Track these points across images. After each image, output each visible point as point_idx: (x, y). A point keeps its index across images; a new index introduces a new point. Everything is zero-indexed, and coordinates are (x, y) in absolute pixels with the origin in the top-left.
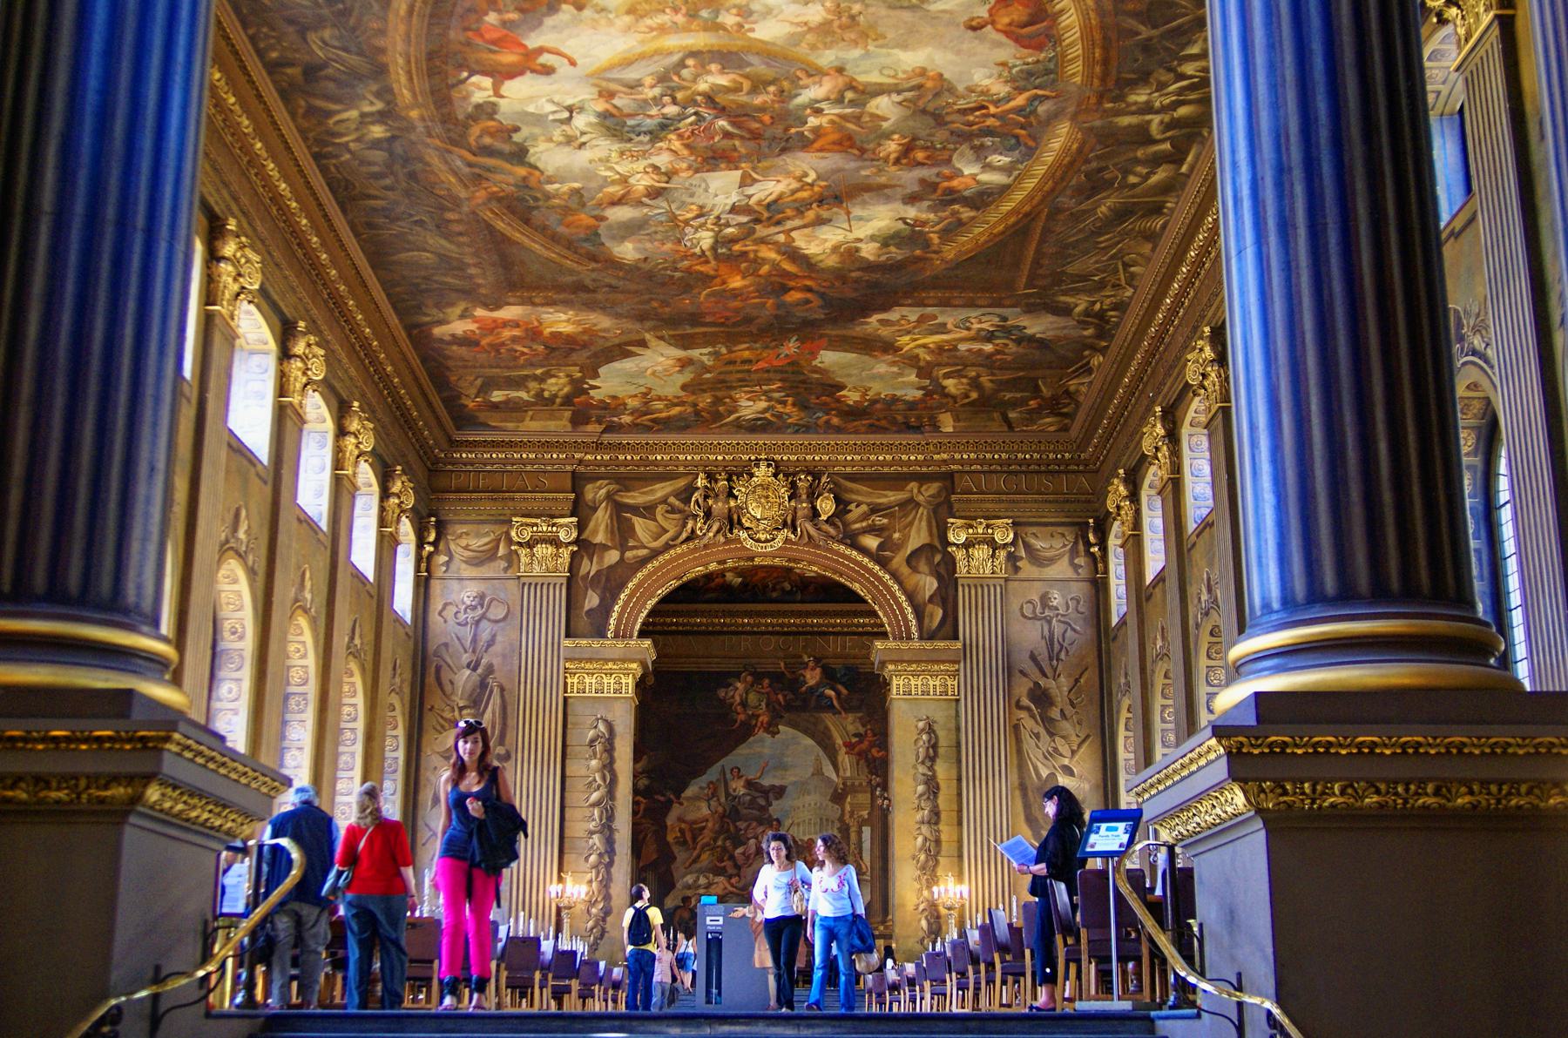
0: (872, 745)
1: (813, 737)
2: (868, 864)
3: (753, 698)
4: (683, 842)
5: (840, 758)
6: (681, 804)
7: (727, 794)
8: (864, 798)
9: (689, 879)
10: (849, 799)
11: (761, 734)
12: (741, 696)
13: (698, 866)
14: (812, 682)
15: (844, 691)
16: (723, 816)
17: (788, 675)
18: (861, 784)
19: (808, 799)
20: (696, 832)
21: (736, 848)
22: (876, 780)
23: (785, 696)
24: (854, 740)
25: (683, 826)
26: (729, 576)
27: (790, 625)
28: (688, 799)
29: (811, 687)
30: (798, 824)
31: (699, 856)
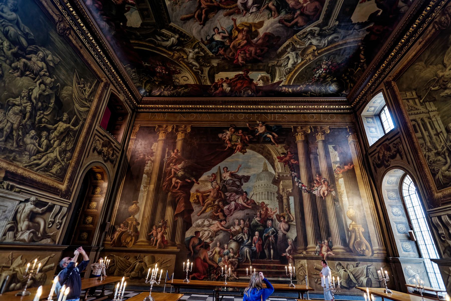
0: (291, 158)
1: (262, 154)
2: (294, 216)
3: (234, 138)
4: (197, 203)
5: (276, 164)
7: (221, 179)
8: (289, 182)
9: (200, 222)
10: (281, 183)
11: (238, 153)
12: (229, 137)
13: (204, 215)
14: (261, 132)
15: (276, 135)
16: (219, 190)
18: (287, 176)
19: (262, 182)
20: (205, 197)
21: (224, 205)
22: (295, 174)
23: (249, 137)
24: (282, 156)
25: (199, 194)
26: (225, 85)
27: (250, 109)
28: (202, 181)
29: (261, 134)
30: (256, 194)
31: (205, 210)
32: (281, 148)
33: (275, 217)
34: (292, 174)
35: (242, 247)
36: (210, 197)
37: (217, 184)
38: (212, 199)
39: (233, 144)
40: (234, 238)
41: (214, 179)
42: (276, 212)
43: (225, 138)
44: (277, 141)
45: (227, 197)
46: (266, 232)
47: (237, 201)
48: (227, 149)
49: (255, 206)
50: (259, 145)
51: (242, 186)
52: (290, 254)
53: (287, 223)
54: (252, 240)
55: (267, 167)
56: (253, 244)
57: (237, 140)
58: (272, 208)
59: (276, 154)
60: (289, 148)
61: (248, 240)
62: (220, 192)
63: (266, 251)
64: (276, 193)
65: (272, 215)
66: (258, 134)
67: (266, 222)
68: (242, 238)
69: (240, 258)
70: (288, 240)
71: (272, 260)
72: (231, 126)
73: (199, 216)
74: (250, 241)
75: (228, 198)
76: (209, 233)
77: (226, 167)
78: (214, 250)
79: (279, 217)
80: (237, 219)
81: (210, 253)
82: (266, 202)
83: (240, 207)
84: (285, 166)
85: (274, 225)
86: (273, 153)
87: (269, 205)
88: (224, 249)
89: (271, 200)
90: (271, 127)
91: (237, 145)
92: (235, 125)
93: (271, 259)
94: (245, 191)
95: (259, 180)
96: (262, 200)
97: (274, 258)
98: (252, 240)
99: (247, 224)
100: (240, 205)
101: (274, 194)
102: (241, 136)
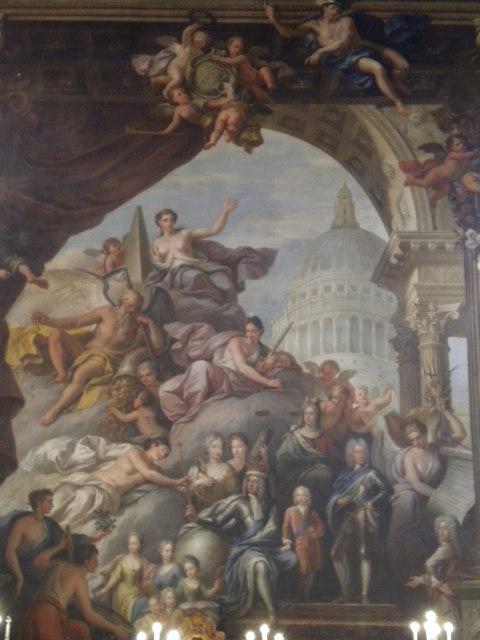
1: (332, 149)
2: (466, 420)
3: (206, 75)
4: (41, 367)
5: (393, 195)
6: (44, 285)
7: (147, 265)
9: (51, 450)
10: (415, 278)
12: (182, 71)
15: (401, 62)
16: (137, 310)
17: (281, 30)
18: (441, 248)
19: (326, 278)
21: (161, 378)
23: (274, 72)
25: (45, 331)
29: (330, 55)
30: (303, 329)
31: (76, 398)
32: (423, 120)
33: (380, 424)
34: (464, 239)
35: (235, 550)
36: (96, 343)
37: (130, 286)
38: (107, 350)
39: (200, 102)
40: (204, 515)
41: (114, 265)
42: (387, 403)
43: (162, 78)
44: (403, 88)
45: (174, 341)
46: (341, 489)
47: (216, 357)
48: (171, 127)
49: (293, 378)
50: (319, 109)
51: (241, 297)
52: (442, 578)
53: (433, 448)
54: (280, 522)
55: (352, 207)
56: (286, 541)
57: (221, 87)
58: (370, 386)
59: (394, 151)
60: (456, 120)
61: (264, 522)
62: (140, 318)
63: (341, 569)
64: (387, 325)
65: (370, 415)
66: (315, 57)
67: (341, 445)
68: (237, 513)
69: (227, 598)
70: (439, 519)
71: (365, 603)
72: (193, 20)
73: (47, 424)
74: (270, 526)
75: (177, 346)
76: (92, 499)
77: (169, 212)
78: (114, 567)
79: (399, 428)
80: (217, 435)
81: (98, 581)
82: (345, 362)
83: (230, 386)
84: (433, 206)
85: (376, 460)
86: (381, 144)
87: (353, 373)
88: (158, 561)
89: (365, 352)
90: (379, 20)
91: (218, 109)
92: (211, 16)
93: (359, 601)
94: (251, 314)
95: (314, 269)
96: (328, 351)
97: (371, 596)
98: (280, 522)
99: (260, 457)
100: (232, 377)
101: (379, 326)
102: (238, 66)
